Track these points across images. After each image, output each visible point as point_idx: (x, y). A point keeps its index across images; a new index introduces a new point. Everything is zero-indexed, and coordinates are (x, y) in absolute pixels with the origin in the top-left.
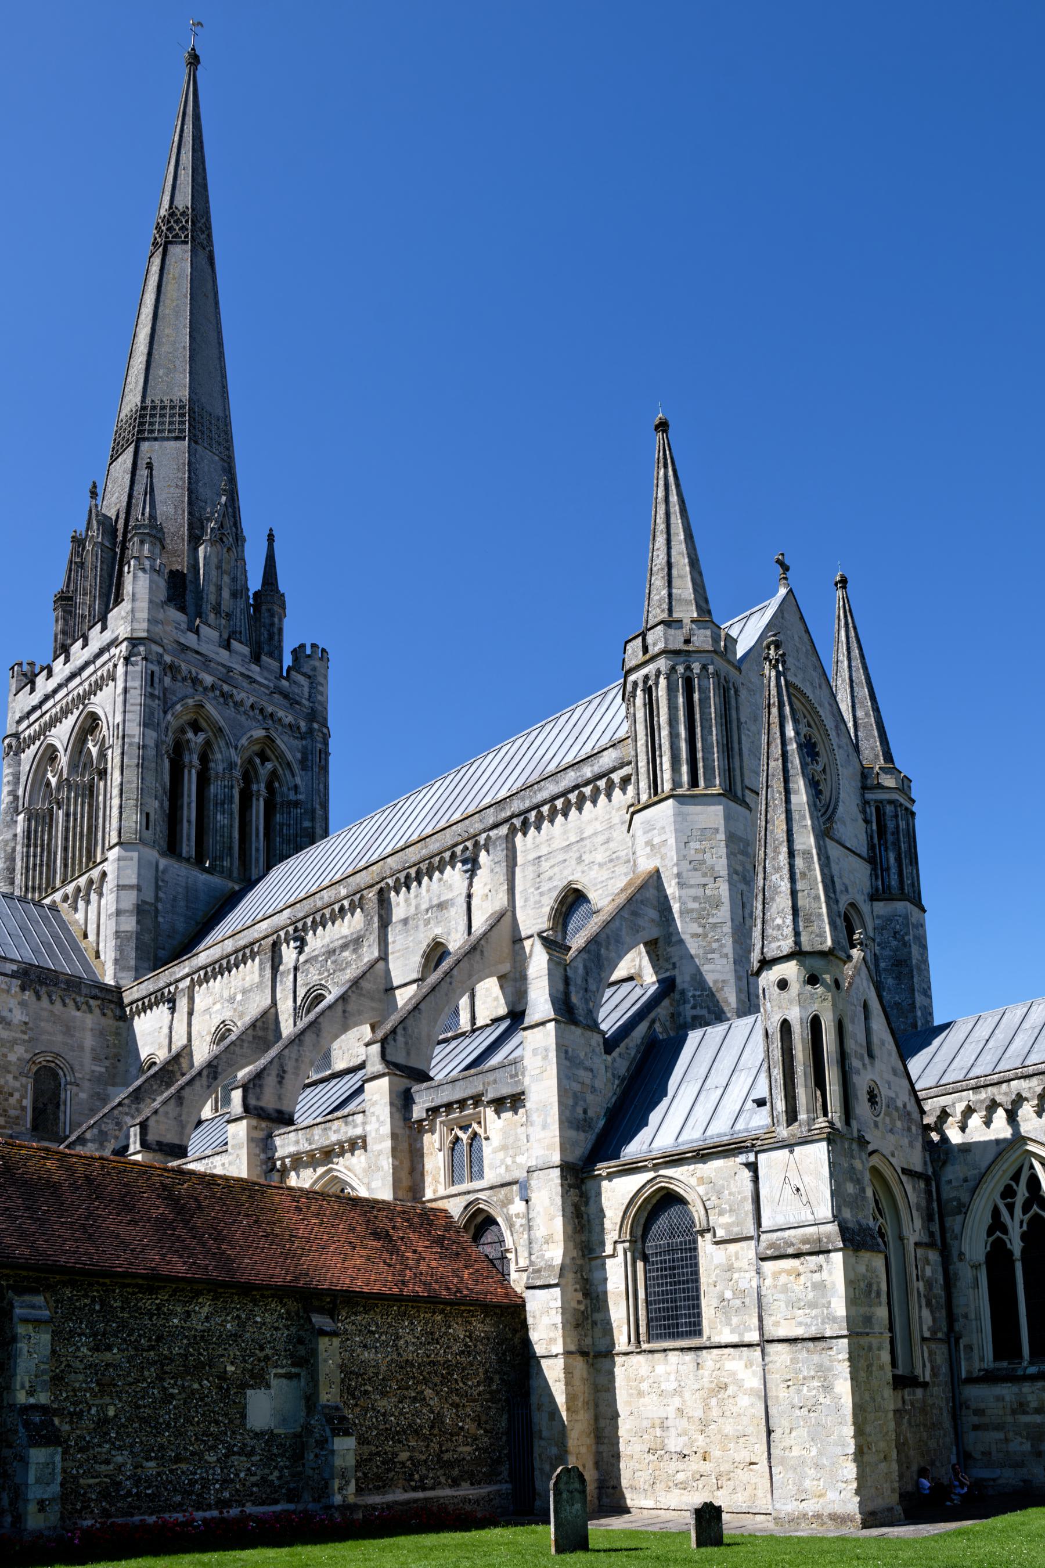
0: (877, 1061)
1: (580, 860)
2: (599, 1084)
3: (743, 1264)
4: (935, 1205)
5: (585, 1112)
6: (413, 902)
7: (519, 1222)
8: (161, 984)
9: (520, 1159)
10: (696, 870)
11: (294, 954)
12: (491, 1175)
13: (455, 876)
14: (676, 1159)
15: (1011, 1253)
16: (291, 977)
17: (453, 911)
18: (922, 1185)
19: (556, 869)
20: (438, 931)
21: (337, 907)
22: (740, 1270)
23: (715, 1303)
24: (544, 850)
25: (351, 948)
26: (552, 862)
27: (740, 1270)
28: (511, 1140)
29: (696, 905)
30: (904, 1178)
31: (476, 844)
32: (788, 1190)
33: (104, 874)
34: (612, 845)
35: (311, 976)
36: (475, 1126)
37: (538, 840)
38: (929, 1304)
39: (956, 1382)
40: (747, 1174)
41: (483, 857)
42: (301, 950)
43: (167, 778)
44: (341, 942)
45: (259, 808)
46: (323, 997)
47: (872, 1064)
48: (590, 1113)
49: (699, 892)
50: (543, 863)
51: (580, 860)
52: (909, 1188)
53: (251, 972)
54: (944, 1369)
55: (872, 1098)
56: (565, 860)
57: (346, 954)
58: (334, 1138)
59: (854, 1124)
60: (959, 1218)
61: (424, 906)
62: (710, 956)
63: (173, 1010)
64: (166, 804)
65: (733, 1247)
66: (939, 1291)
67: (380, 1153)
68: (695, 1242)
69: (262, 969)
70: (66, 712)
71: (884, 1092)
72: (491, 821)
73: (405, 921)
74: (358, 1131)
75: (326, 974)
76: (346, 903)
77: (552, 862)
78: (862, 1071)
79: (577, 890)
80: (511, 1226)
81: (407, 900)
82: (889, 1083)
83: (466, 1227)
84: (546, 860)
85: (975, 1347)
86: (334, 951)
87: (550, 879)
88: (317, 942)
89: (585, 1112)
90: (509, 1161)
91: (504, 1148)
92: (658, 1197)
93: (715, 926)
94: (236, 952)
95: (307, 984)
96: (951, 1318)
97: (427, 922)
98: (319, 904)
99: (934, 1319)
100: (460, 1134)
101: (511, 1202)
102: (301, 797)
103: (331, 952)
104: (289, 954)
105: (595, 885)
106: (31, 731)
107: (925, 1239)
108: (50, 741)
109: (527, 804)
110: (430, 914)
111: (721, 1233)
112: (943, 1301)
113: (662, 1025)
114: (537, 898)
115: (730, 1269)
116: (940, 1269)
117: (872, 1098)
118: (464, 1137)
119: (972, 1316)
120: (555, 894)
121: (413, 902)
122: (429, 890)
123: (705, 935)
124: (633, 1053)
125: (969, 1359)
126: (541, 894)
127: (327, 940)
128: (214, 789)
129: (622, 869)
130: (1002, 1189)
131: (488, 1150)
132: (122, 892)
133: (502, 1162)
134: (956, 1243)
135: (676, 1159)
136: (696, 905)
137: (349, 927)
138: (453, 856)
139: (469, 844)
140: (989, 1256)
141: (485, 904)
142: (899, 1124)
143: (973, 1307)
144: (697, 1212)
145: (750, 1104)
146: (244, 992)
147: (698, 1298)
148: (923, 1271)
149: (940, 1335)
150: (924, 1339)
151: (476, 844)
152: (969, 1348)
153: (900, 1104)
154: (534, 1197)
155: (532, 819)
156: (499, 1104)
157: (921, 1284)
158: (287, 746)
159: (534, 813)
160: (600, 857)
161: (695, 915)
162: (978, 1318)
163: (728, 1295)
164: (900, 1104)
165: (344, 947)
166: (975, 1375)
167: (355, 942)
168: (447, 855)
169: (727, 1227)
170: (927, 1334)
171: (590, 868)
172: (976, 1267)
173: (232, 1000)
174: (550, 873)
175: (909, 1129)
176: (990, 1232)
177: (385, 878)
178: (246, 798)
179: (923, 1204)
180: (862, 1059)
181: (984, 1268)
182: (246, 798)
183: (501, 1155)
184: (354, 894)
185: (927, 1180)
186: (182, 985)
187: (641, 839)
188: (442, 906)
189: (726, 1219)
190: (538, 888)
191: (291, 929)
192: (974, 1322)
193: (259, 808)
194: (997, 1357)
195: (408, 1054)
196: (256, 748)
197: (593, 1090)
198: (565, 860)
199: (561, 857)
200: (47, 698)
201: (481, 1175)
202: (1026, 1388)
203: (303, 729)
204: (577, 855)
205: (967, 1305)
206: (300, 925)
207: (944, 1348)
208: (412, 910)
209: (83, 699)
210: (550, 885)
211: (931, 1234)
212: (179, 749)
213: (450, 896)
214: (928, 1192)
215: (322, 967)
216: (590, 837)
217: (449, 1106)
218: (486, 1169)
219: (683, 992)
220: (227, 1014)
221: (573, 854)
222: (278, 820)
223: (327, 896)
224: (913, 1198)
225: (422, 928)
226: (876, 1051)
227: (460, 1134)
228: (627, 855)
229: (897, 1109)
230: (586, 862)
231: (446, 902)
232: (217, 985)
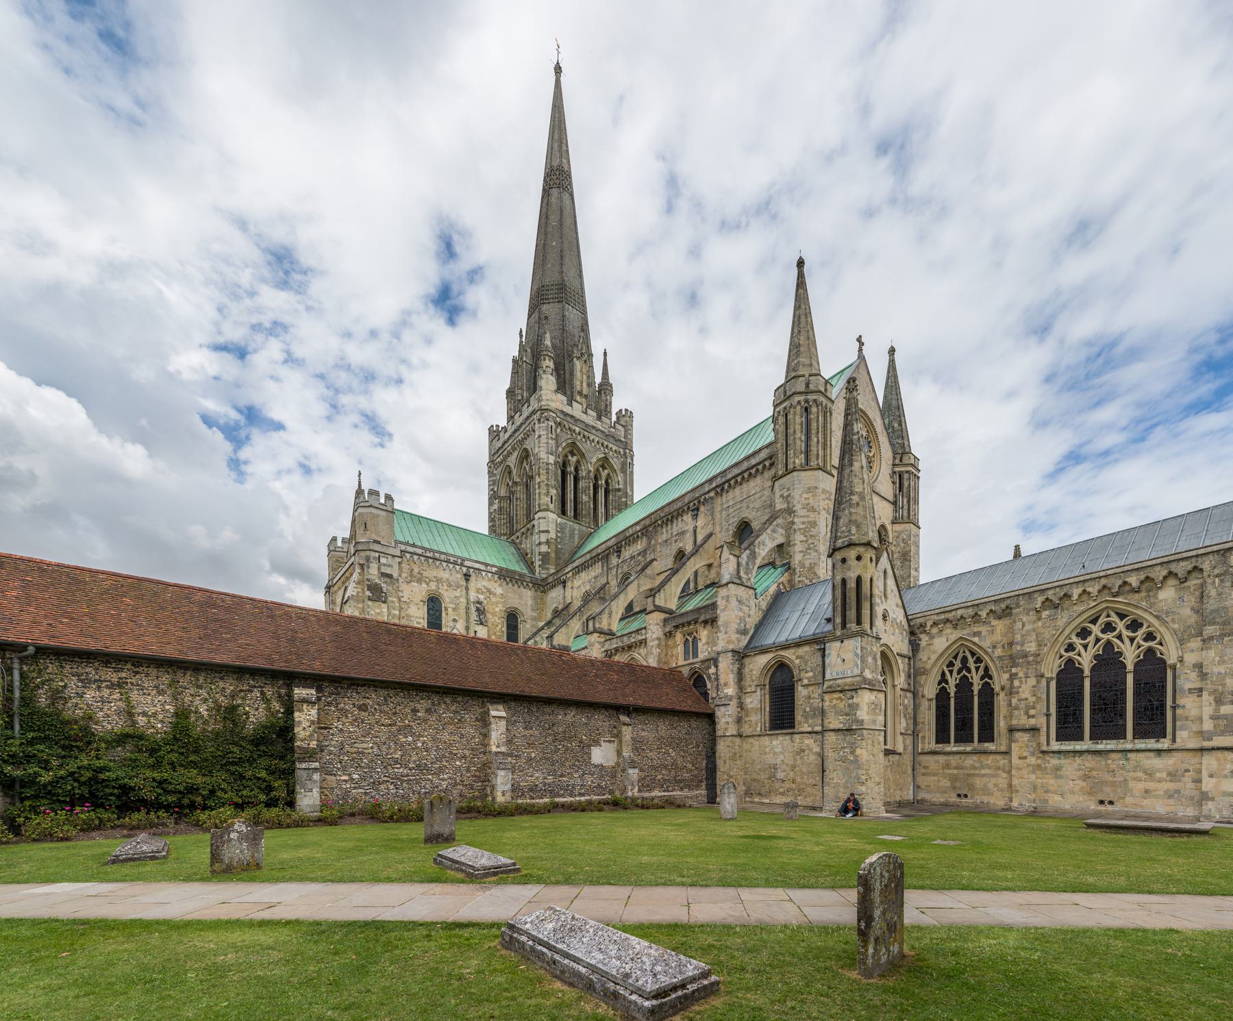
0: (888, 601)
1: (748, 507)
2: (752, 613)
3: (816, 695)
4: (912, 670)
5: (745, 626)
7: (713, 677)
8: (559, 575)
9: (714, 648)
12: (701, 656)
13: (688, 518)
14: (785, 647)
15: (949, 694)
17: (688, 534)
18: (907, 660)
19: (736, 512)
20: (681, 545)
21: (635, 536)
22: (814, 698)
23: (801, 713)
26: (735, 508)
27: (814, 698)
28: (710, 640)
29: (803, 526)
30: (897, 657)
31: (699, 502)
32: (839, 659)
33: (534, 526)
34: (764, 498)
35: (625, 569)
36: (695, 633)
38: (905, 716)
39: (916, 754)
40: (819, 654)
41: (702, 509)
42: (619, 557)
43: (560, 479)
46: (629, 578)
47: (886, 601)
48: (748, 627)
49: (805, 520)
51: (748, 507)
52: (900, 661)
53: (597, 569)
54: (910, 748)
55: (885, 617)
57: (639, 558)
58: (633, 640)
59: (874, 629)
60: (924, 677)
61: (674, 534)
63: (564, 587)
64: (560, 491)
65: (811, 688)
66: (910, 710)
67: (652, 647)
68: (794, 685)
69: (603, 567)
70: (514, 449)
71: (891, 614)
72: (706, 490)
73: (666, 541)
74: (643, 637)
77: (735, 508)
78: (881, 605)
79: (746, 522)
80: (710, 678)
81: (667, 531)
82: (894, 611)
83: (690, 680)
87: (734, 517)
88: (627, 553)
89: (745, 626)
90: (710, 649)
91: (707, 643)
92: (777, 665)
93: (811, 536)
94: (591, 558)
96: (915, 723)
97: (676, 541)
99: (907, 724)
100: (688, 638)
101: (710, 668)
102: (621, 486)
103: (632, 557)
104: (614, 560)
106: (499, 459)
107: (906, 687)
108: (508, 463)
109: (724, 480)
111: (806, 682)
112: (912, 716)
113: (784, 585)
115: (809, 697)
116: (912, 701)
117: (885, 617)
118: (690, 639)
121: (670, 532)
122: (677, 527)
123: (807, 541)
124: (769, 598)
125: (923, 743)
128: (582, 484)
129: (767, 511)
131: (700, 645)
132: (542, 534)
133: (707, 650)
134: (921, 689)
135: (785, 647)
136: (803, 526)
138: (689, 508)
139: (696, 502)
140: (937, 695)
141: (703, 531)
142: (897, 631)
144: (796, 672)
145: (823, 621)
146: (595, 578)
147: (794, 711)
148: (903, 701)
149: (909, 732)
150: (901, 734)
151: (699, 502)
152: (924, 738)
153: (898, 621)
154: (721, 665)
155: (726, 487)
156: (705, 622)
157: (901, 707)
158: (616, 462)
159: (727, 485)
160: (757, 504)
162: (929, 724)
163: (808, 709)
164: (898, 621)
165: (639, 554)
168: (686, 508)
169: (809, 679)
170: (903, 731)
172: (929, 700)
173: (589, 581)
174: (734, 514)
175: (902, 634)
176: (939, 684)
179: (907, 669)
180: (881, 598)
181: (934, 701)
183: (706, 646)
185: (909, 658)
186: (568, 576)
187: (778, 494)
188: (683, 533)
189: (811, 674)
191: (615, 547)
194: (937, 743)
195: (666, 601)
196: (600, 463)
197: (749, 616)
199: (738, 506)
200: (505, 442)
201: (697, 657)
202: (951, 758)
203: (622, 453)
205: (924, 718)
206: (619, 545)
207: (911, 738)
208: (669, 536)
209: (522, 442)
211: (909, 684)
212: (565, 464)
214: (909, 664)
217: (683, 625)
218: (699, 654)
219: (794, 570)
220: (588, 588)
221: (744, 504)
223: (631, 531)
224: (901, 666)
225: (674, 544)
226: (889, 596)
227: (688, 638)
229: (897, 623)
231: (684, 531)
232: (583, 575)
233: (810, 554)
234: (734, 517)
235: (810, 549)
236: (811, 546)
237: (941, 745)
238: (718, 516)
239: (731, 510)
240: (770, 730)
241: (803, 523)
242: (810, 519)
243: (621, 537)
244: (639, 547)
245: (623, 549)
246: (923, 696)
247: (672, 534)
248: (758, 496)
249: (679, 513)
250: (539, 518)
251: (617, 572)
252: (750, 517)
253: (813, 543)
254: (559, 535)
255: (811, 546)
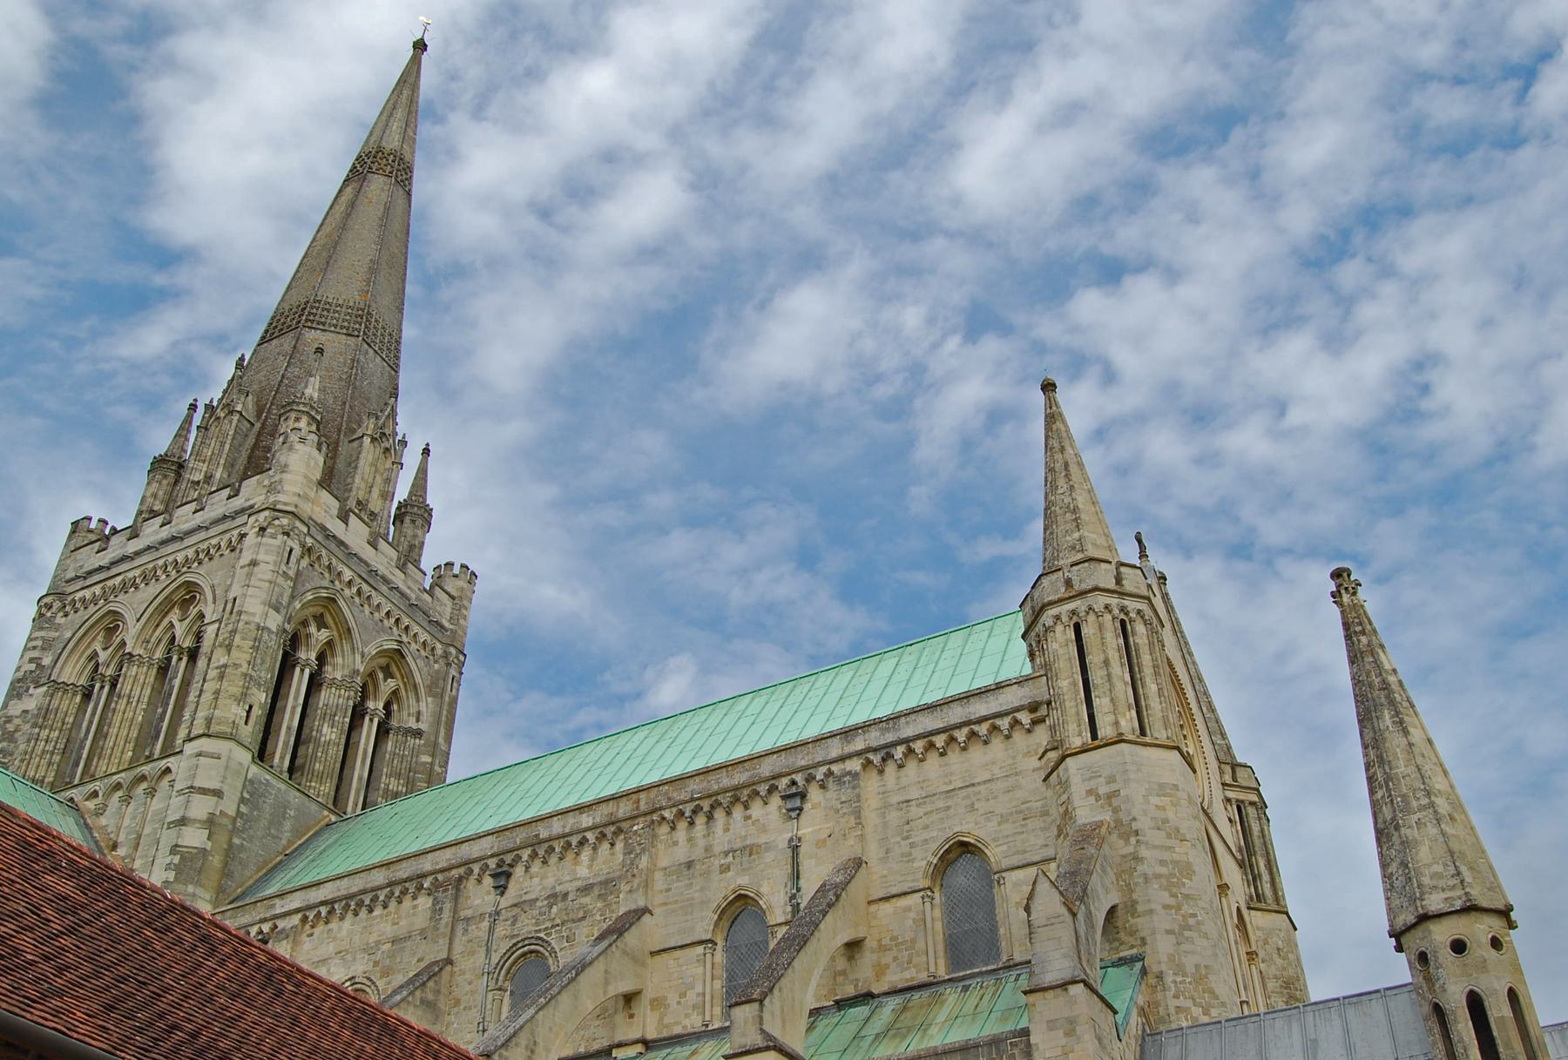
1: (972, 808)
6: (701, 843)
10: (1158, 829)
11: (492, 897)
13: (769, 812)
16: (485, 924)
17: (769, 857)
19: (935, 817)
20: (743, 880)
21: (574, 840)
24: (914, 793)
25: (596, 891)
37: (904, 781)
41: (814, 793)
44: (579, 884)
45: (368, 731)
50: (913, 809)
56: (948, 808)
57: (586, 900)
62: (1187, 934)
73: (689, 865)
75: (549, 924)
76: (590, 836)
84: (918, 805)
86: (566, 894)
87: (926, 827)
88: (530, 882)
95: (513, 936)
97: (725, 869)
98: (544, 834)
104: (480, 896)
105: (994, 840)
110: (730, 858)
114: (907, 849)
120: (934, 846)
122: (729, 830)
123: (1179, 908)
126: (912, 845)
127: (550, 881)
137: (590, 867)
161: (1164, 881)
165: (586, 889)
167: (607, 886)
171: (988, 820)
174: (926, 820)
177: (661, 809)
178: (358, 714)
182: (358, 714)
184: (606, 825)
190: (907, 838)
191: (492, 863)
193: (368, 731)
198: (948, 808)
199: (941, 804)
204: (968, 802)
206: (508, 858)
210: (925, 835)
213: (763, 839)
215: (540, 914)
216: (985, 782)
222: (389, 749)
223: (557, 827)
225: (716, 876)
228: (1043, 806)
230: (981, 811)
233: (1190, 940)
234: (926, 827)
235: (1190, 928)
236: (1191, 921)
238: (871, 818)
239: (915, 811)
241: (1162, 863)
242: (1176, 857)
243: (520, 837)
244: (583, 871)
245: (519, 871)
247: (708, 849)
248: (1000, 785)
249: (741, 797)
250: (199, 755)
251: (491, 930)
252: (981, 833)
253: (1194, 915)
254: (243, 809)
255: (1191, 921)
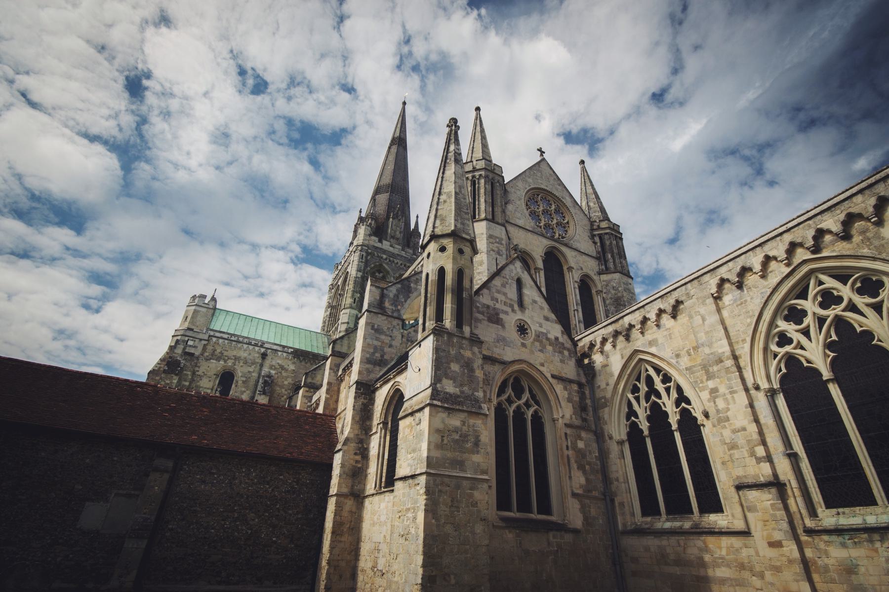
60: (606, 410)
85: (626, 504)
119: (621, 480)
130: (631, 387)
140: (629, 434)
143: (621, 472)
149: (595, 493)
152: (622, 504)
162: (627, 481)
166: (629, 528)
172: (621, 443)
192: (623, 485)
205: (617, 471)
237: (649, 519)
240: (385, 487)
246: (611, 438)
